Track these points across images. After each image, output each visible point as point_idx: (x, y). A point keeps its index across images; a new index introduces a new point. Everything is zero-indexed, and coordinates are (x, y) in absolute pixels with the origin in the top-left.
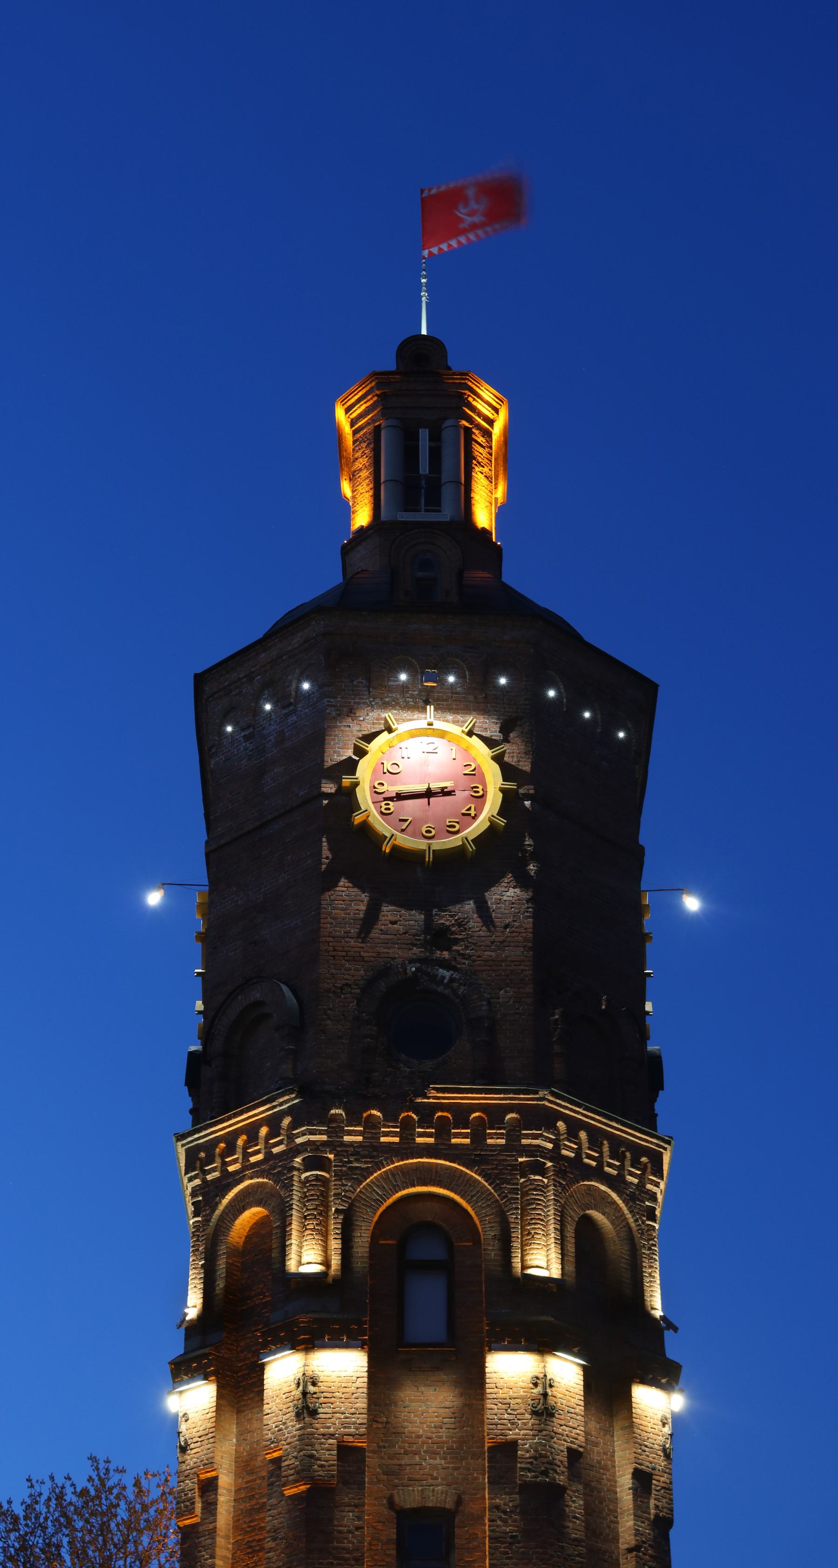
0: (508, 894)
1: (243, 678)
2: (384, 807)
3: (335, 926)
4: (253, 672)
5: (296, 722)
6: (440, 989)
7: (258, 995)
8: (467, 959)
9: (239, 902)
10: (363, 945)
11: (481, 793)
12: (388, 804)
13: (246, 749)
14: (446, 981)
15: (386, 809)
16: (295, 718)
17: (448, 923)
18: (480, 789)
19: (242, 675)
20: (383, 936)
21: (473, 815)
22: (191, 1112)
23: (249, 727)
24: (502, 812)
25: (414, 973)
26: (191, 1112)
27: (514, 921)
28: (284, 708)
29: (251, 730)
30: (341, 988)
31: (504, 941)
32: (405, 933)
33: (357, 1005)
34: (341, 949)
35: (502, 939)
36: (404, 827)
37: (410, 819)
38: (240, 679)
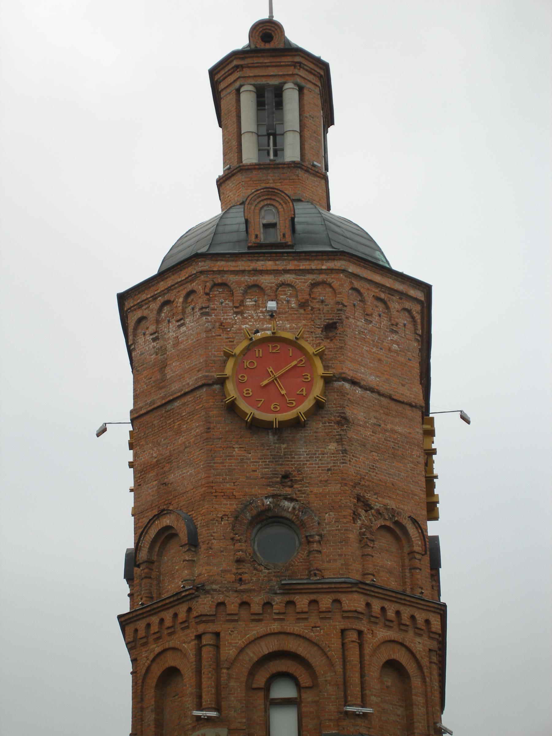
0: (329, 447)
1: (150, 298)
2: (246, 392)
3: (216, 475)
4: (156, 294)
5: (185, 332)
6: (285, 514)
7: (168, 522)
8: (303, 493)
9: (154, 455)
10: (235, 487)
11: (310, 379)
12: (248, 390)
13: (154, 347)
14: (290, 510)
15: (246, 394)
16: (185, 328)
17: (290, 470)
18: (309, 375)
19: (149, 296)
20: (247, 481)
21: (304, 395)
22: (129, 595)
23: (155, 333)
25: (269, 505)
26: (129, 595)
27: (335, 466)
28: (178, 321)
29: (157, 334)
30: (222, 518)
31: (328, 480)
32: (262, 478)
33: (233, 529)
34: (220, 491)
35: (326, 478)
36: (259, 406)
37: (263, 400)
38: (147, 299)
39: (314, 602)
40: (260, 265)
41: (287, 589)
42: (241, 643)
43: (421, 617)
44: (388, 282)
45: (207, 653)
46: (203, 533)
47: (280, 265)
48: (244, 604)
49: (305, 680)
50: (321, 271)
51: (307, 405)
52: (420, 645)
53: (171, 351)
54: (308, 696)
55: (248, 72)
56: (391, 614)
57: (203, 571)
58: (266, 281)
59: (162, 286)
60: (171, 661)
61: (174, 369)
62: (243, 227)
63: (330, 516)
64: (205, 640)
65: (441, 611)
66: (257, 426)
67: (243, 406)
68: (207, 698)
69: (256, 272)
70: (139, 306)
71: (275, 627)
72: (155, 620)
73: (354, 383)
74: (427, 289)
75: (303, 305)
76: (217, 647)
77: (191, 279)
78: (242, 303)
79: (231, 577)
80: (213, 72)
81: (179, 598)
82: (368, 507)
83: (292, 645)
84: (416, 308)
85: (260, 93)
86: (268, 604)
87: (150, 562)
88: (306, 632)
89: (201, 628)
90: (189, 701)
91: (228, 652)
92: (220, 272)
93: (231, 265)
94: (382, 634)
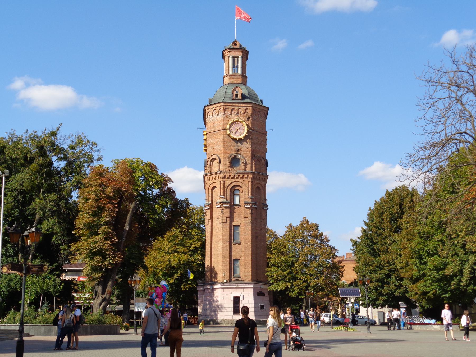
24: (247, 133)
39: (243, 176)
40: (235, 104)
41: (239, 173)
42: (229, 183)
43: (263, 178)
44: (260, 108)
45: (222, 185)
46: (222, 161)
47: (239, 105)
48: (230, 176)
49: (241, 191)
50: (247, 106)
51: (244, 135)
52: (263, 183)
53: (216, 120)
54: (241, 194)
55: (231, 53)
56: (258, 178)
57: (221, 168)
58: (236, 108)
59: (214, 106)
60: (214, 185)
61: (216, 124)
62: (231, 94)
63: (247, 159)
64: (222, 182)
65: (268, 176)
66: (234, 139)
67: (231, 135)
68: (222, 193)
69: (234, 106)
70: (209, 109)
71: (236, 180)
72: (211, 176)
73: (253, 130)
74: (268, 108)
75: (244, 113)
76: (224, 184)
77: (220, 106)
78: (231, 113)
79: (227, 170)
80: (223, 51)
81: (217, 173)
82: (254, 156)
83: (239, 184)
84: (266, 112)
85: (234, 58)
86: (234, 176)
87: (210, 164)
88: (242, 181)
89: (221, 180)
90: (219, 194)
91: (226, 185)
92: (227, 106)
93: (229, 104)
94: (256, 182)
